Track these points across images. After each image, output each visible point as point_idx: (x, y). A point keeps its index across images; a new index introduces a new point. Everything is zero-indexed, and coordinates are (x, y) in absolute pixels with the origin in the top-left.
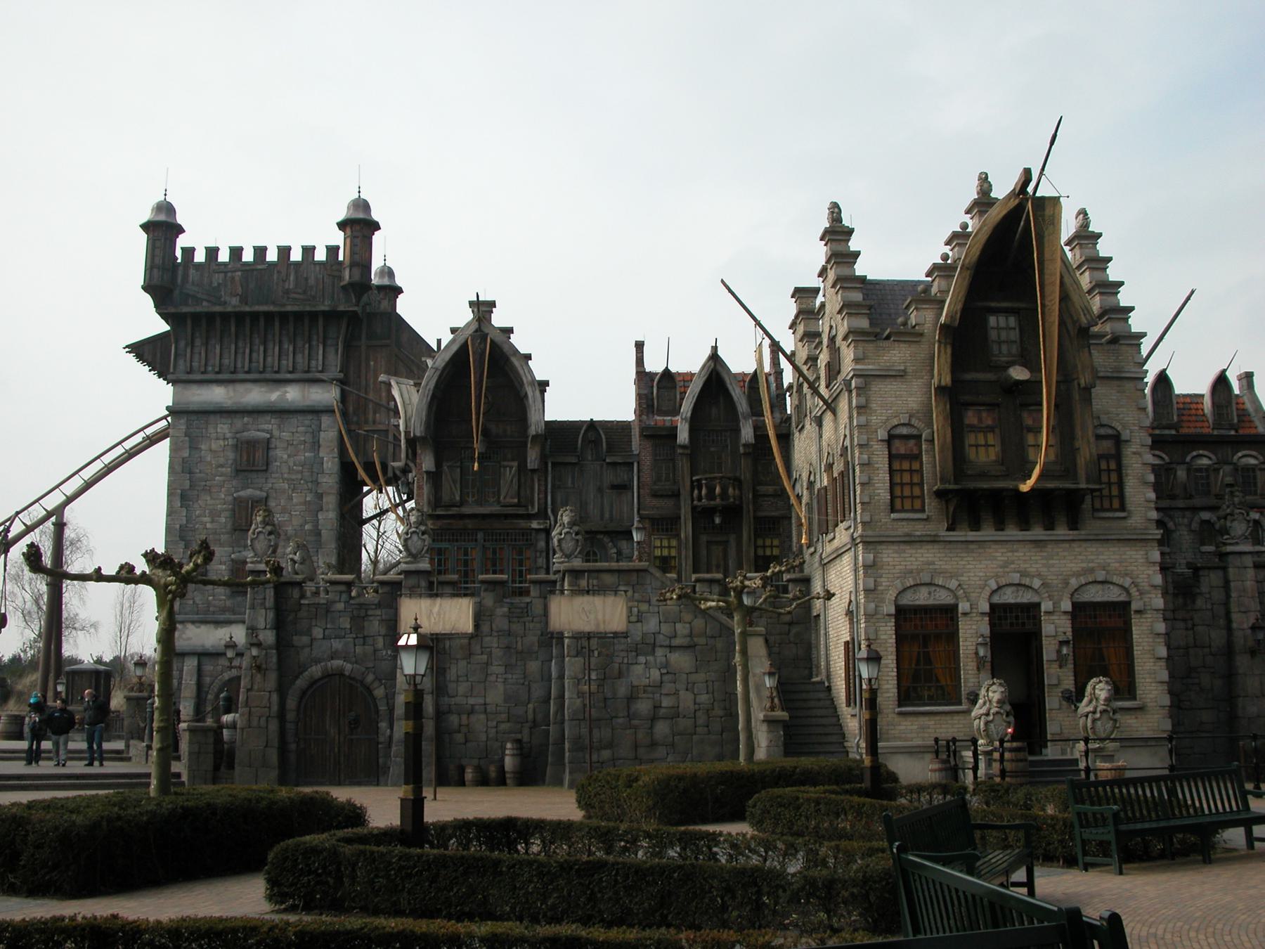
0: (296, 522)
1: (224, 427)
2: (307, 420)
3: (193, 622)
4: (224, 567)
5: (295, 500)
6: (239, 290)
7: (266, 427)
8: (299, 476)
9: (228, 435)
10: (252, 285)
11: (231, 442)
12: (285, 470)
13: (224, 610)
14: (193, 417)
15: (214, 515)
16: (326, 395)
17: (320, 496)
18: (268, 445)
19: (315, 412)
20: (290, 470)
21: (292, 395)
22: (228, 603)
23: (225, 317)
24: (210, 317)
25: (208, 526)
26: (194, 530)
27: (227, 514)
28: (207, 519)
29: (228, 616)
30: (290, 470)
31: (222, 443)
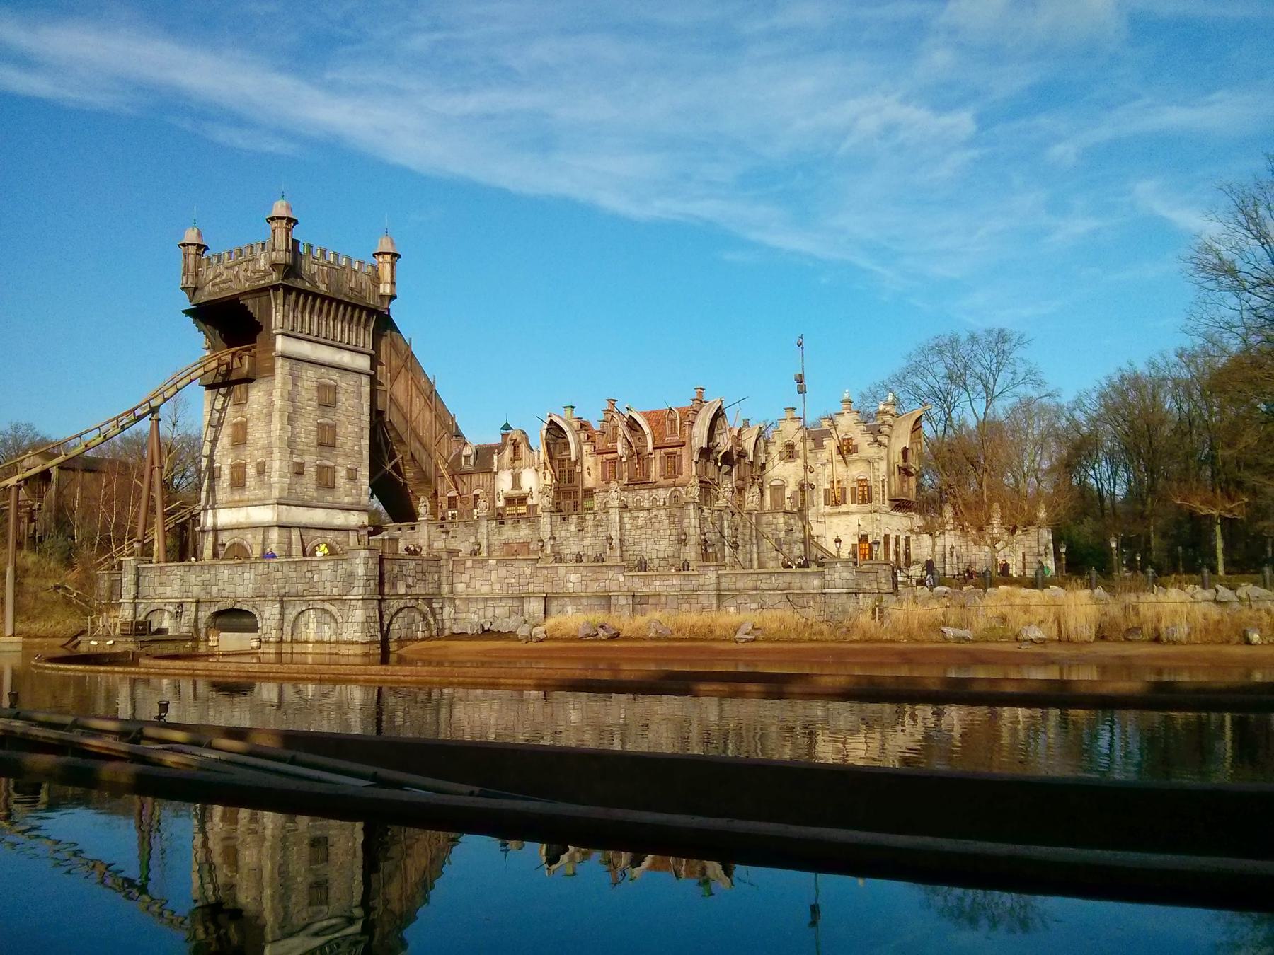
0: (350, 444)
1: (310, 373)
2: (357, 375)
3: (296, 506)
4: (312, 469)
5: (349, 430)
6: (326, 281)
7: (333, 377)
8: (351, 414)
9: (314, 379)
10: (333, 279)
11: (315, 384)
12: (344, 409)
13: (313, 498)
14: (294, 362)
15: (307, 434)
16: (363, 363)
17: (362, 429)
18: (334, 389)
19: (360, 372)
20: (347, 410)
21: (346, 358)
22: (315, 495)
23: (316, 296)
24: (307, 293)
25: (303, 440)
26: (296, 442)
27: (314, 433)
28: (303, 435)
29: (315, 503)
30: (347, 410)
31: (310, 384)
